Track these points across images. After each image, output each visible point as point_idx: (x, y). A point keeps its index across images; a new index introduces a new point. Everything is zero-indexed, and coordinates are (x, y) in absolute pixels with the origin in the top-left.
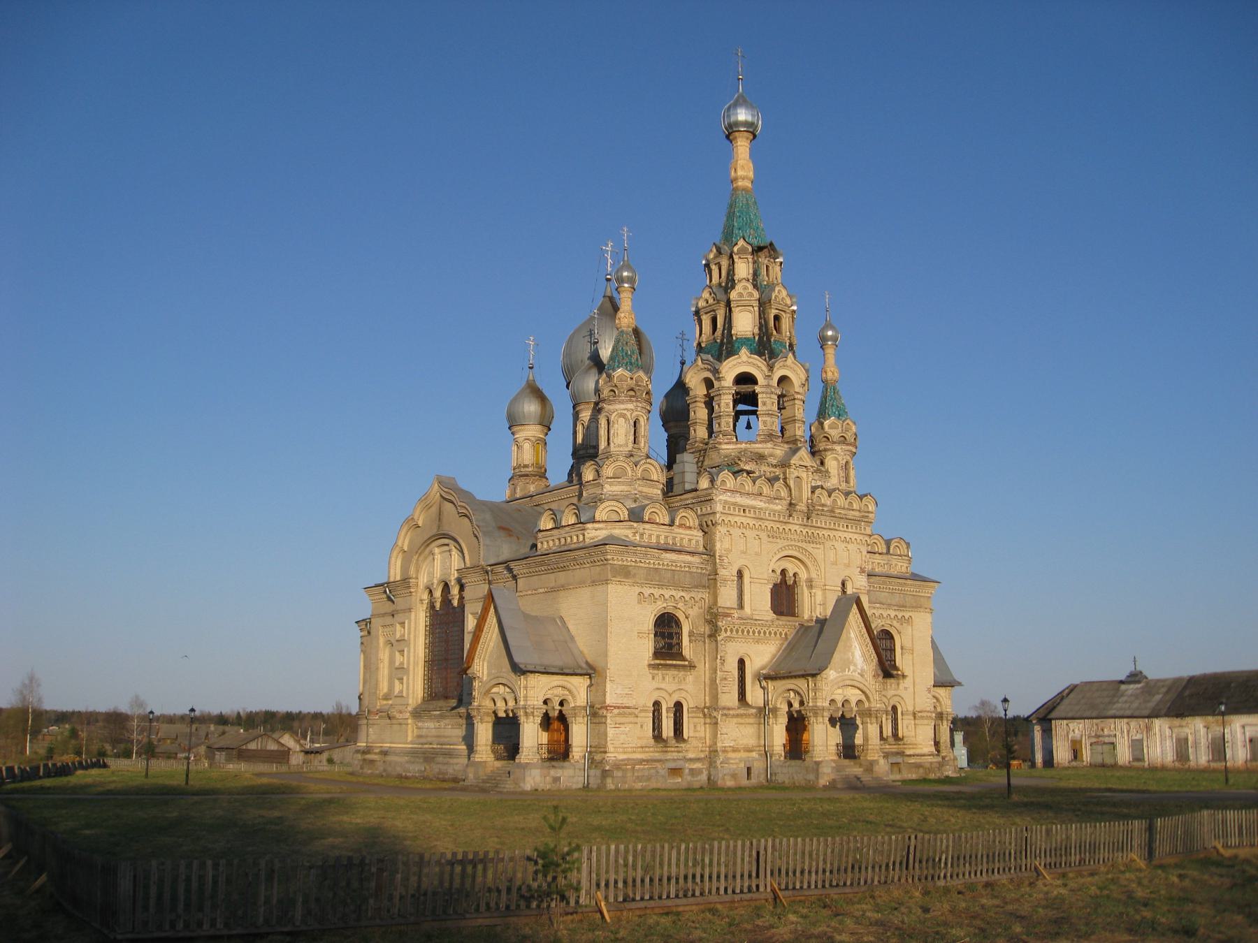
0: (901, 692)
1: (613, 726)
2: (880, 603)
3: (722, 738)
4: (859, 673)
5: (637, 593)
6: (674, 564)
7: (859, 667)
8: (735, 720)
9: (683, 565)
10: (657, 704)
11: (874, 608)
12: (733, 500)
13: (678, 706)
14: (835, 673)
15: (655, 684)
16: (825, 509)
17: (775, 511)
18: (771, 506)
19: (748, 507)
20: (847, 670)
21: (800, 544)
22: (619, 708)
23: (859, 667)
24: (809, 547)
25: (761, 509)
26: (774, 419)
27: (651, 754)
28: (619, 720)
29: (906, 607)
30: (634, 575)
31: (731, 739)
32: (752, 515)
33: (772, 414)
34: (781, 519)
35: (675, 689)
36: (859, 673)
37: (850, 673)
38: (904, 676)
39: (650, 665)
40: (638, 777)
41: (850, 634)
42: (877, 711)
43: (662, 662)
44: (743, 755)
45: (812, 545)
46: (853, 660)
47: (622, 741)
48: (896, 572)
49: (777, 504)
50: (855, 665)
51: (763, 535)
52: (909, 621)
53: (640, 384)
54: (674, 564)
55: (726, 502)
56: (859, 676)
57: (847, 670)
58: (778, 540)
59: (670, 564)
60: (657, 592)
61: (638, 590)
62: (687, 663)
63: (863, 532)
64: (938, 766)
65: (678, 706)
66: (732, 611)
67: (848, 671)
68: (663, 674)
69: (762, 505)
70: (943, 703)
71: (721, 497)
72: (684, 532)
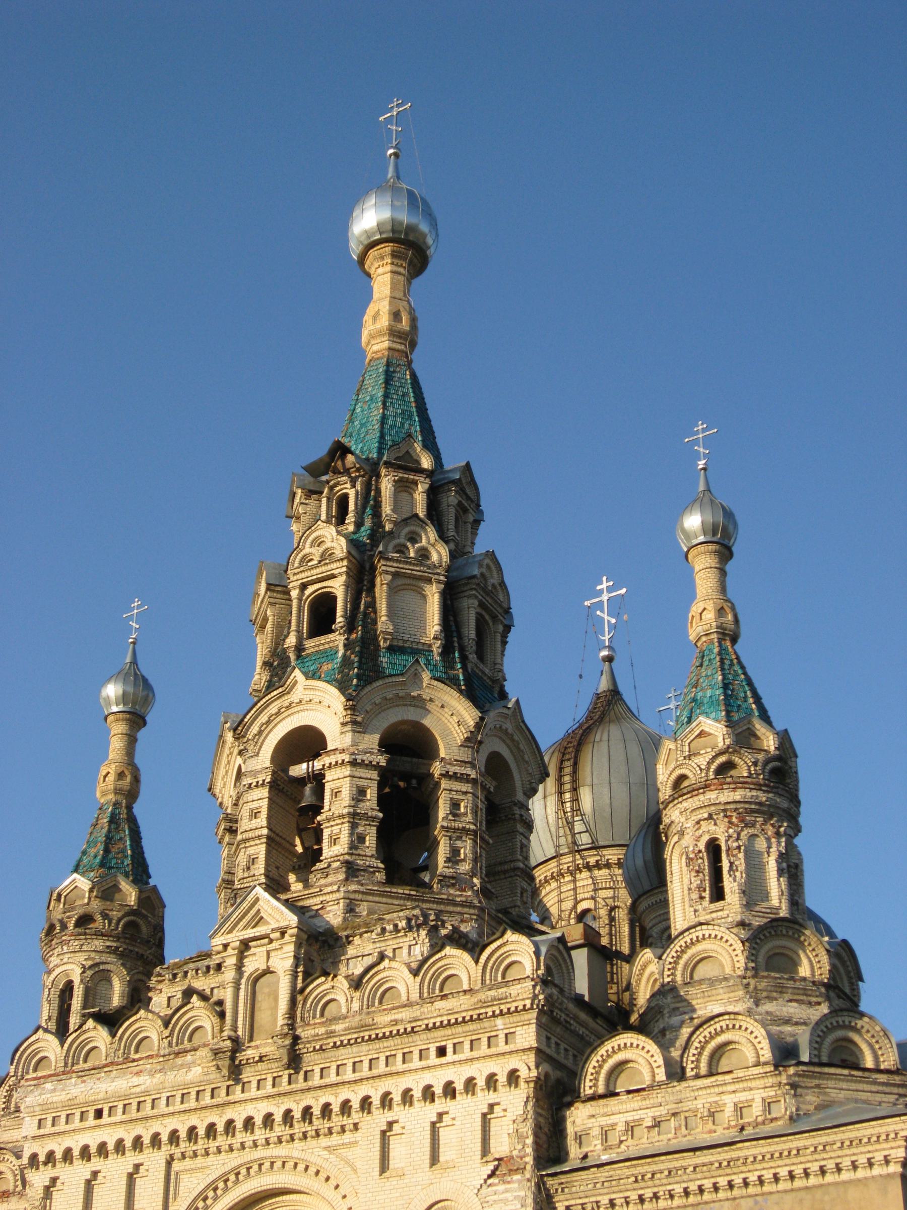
16: (339, 1027)
25: (146, 1093)
45: (324, 1141)
48: (720, 1130)
49: (189, 1067)
53: (78, 903)
69: (145, 1082)
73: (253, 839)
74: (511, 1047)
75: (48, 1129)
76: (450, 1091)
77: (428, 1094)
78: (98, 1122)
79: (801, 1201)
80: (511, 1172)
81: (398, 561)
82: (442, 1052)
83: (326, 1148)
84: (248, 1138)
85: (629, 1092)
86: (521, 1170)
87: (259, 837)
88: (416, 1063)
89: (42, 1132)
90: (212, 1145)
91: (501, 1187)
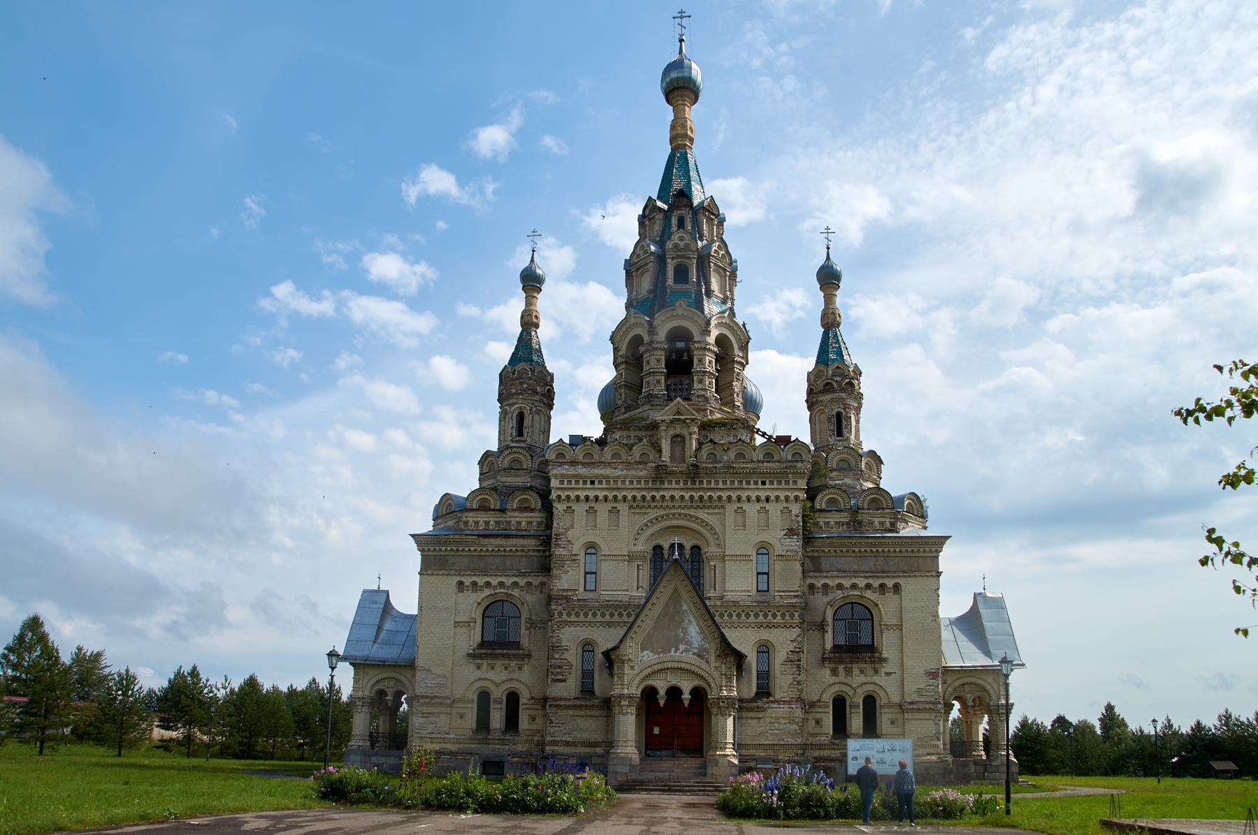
0: (881, 680)
1: (421, 715)
2: (839, 571)
3: (552, 731)
4: (694, 654)
5: (455, 582)
6: (502, 549)
7: (695, 645)
8: (571, 712)
9: (514, 549)
10: (484, 699)
11: (826, 577)
12: (574, 472)
13: (513, 699)
14: (650, 654)
15: (478, 674)
17: (639, 477)
18: (633, 473)
19: (597, 477)
20: (673, 649)
21: (686, 511)
22: (427, 697)
23: (695, 645)
24: (702, 514)
25: (618, 477)
26: (657, 378)
27: (466, 746)
28: (426, 709)
29: (887, 572)
30: (453, 564)
31: (564, 732)
32: (604, 486)
33: (653, 372)
34: (650, 485)
35: (504, 678)
36: (694, 654)
37: (678, 654)
38: (882, 660)
39: (469, 655)
40: (442, 767)
41: (681, 606)
42: (719, 699)
43: (488, 651)
44: (580, 750)
45: (706, 511)
46: (684, 637)
47: (430, 731)
50: (689, 643)
51: (623, 508)
52: (897, 588)
54: (502, 549)
55: (563, 476)
56: (695, 657)
57: (673, 649)
58: (649, 511)
59: (496, 549)
60: (481, 581)
61: (456, 579)
62: (521, 652)
63: (791, 486)
64: (941, 772)
65: (513, 699)
66: (570, 593)
67: (675, 652)
68: (489, 664)
69: (618, 473)
70: (992, 692)
71: (554, 472)
72: (520, 515)
73: (658, 372)
74: (795, 487)
75: (565, 485)
76: (767, 500)
77: (758, 499)
78: (592, 486)
79: (902, 561)
80: (793, 535)
81: (716, 258)
82: (764, 483)
83: (706, 513)
84: (671, 504)
85: (836, 511)
86: (797, 534)
87: (662, 372)
88: (752, 486)
89: (562, 486)
90: (653, 505)
91: (789, 540)
